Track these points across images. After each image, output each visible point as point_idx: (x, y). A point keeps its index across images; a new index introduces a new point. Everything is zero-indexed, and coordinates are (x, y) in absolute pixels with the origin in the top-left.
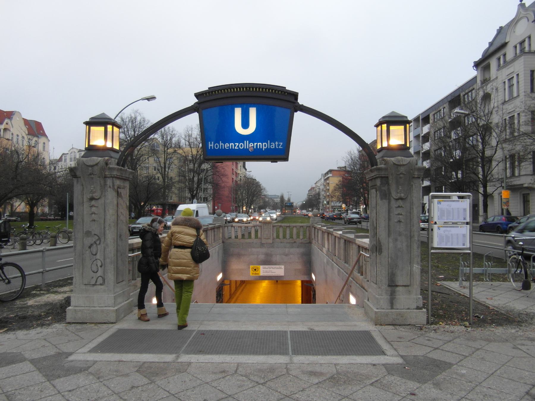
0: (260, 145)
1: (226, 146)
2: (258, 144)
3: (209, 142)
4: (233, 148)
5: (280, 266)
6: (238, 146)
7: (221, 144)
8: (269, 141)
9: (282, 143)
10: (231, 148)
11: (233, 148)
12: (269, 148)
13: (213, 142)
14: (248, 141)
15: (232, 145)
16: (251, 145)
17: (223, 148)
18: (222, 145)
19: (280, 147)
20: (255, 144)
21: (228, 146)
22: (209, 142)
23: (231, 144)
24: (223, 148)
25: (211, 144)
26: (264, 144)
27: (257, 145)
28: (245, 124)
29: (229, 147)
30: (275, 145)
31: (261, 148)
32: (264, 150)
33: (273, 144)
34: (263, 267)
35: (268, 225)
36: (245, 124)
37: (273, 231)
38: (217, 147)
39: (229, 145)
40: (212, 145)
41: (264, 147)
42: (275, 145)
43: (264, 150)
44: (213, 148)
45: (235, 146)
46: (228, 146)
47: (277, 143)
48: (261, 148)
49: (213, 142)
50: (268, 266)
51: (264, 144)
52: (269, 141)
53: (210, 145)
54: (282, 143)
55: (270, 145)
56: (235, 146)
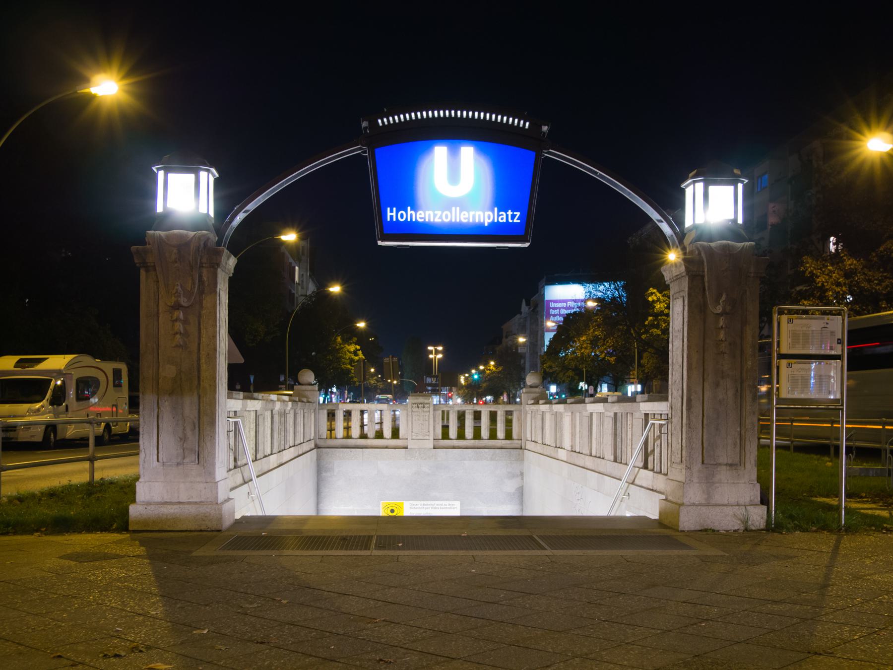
3: (389, 209)
5: (451, 503)
7: (409, 212)
9: (518, 214)
13: (395, 209)
14: (458, 209)
15: (429, 215)
18: (411, 215)
19: (515, 221)
20: (472, 213)
22: (389, 209)
25: (392, 211)
27: (474, 217)
30: (507, 216)
33: (502, 215)
34: (411, 505)
35: (424, 407)
37: (434, 421)
38: (402, 216)
39: (425, 213)
40: (394, 214)
42: (507, 216)
44: (394, 220)
45: (435, 215)
47: (510, 213)
49: (395, 209)
50: (422, 502)
53: (389, 214)
54: (518, 214)
55: (499, 216)
56: (435, 215)
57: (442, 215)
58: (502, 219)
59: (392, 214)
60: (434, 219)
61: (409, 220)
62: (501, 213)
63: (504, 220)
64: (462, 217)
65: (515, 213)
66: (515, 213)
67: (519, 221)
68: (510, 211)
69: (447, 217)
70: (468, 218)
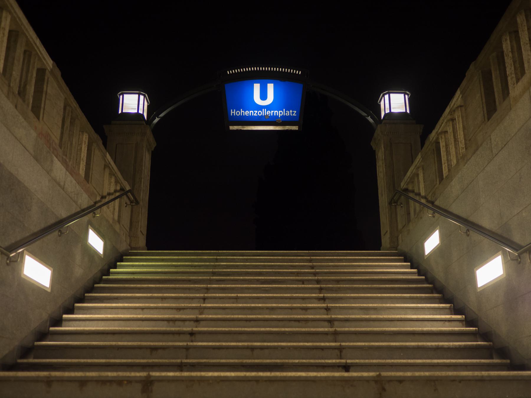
0: (276, 112)
1: (246, 113)
2: (275, 112)
3: (232, 110)
4: (253, 115)
7: (242, 112)
8: (284, 109)
9: (295, 112)
10: (250, 115)
11: (253, 115)
12: (284, 115)
13: (235, 110)
14: (265, 109)
15: (252, 113)
16: (269, 112)
17: (244, 115)
18: (243, 113)
19: (294, 115)
20: (272, 112)
22: (232, 110)
23: (250, 112)
24: (244, 115)
25: (233, 111)
26: (280, 112)
27: (273, 113)
28: (264, 96)
29: (249, 114)
30: (290, 113)
31: (277, 115)
32: (280, 117)
33: (288, 112)
36: (264, 96)
38: (238, 113)
40: (234, 112)
41: (280, 114)
42: (290, 113)
43: (280, 117)
44: (235, 115)
45: (254, 113)
46: (248, 113)
47: (291, 111)
48: (277, 115)
49: (235, 110)
51: (280, 112)
52: (284, 109)
53: (232, 112)
54: (295, 112)
55: (285, 113)
56: (254, 113)
57: (257, 113)
58: (287, 114)
60: (254, 114)
61: (241, 115)
62: (286, 111)
65: (294, 111)
66: (294, 111)
67: (296, 115)
68: (291, 110)
69: (260, 114)
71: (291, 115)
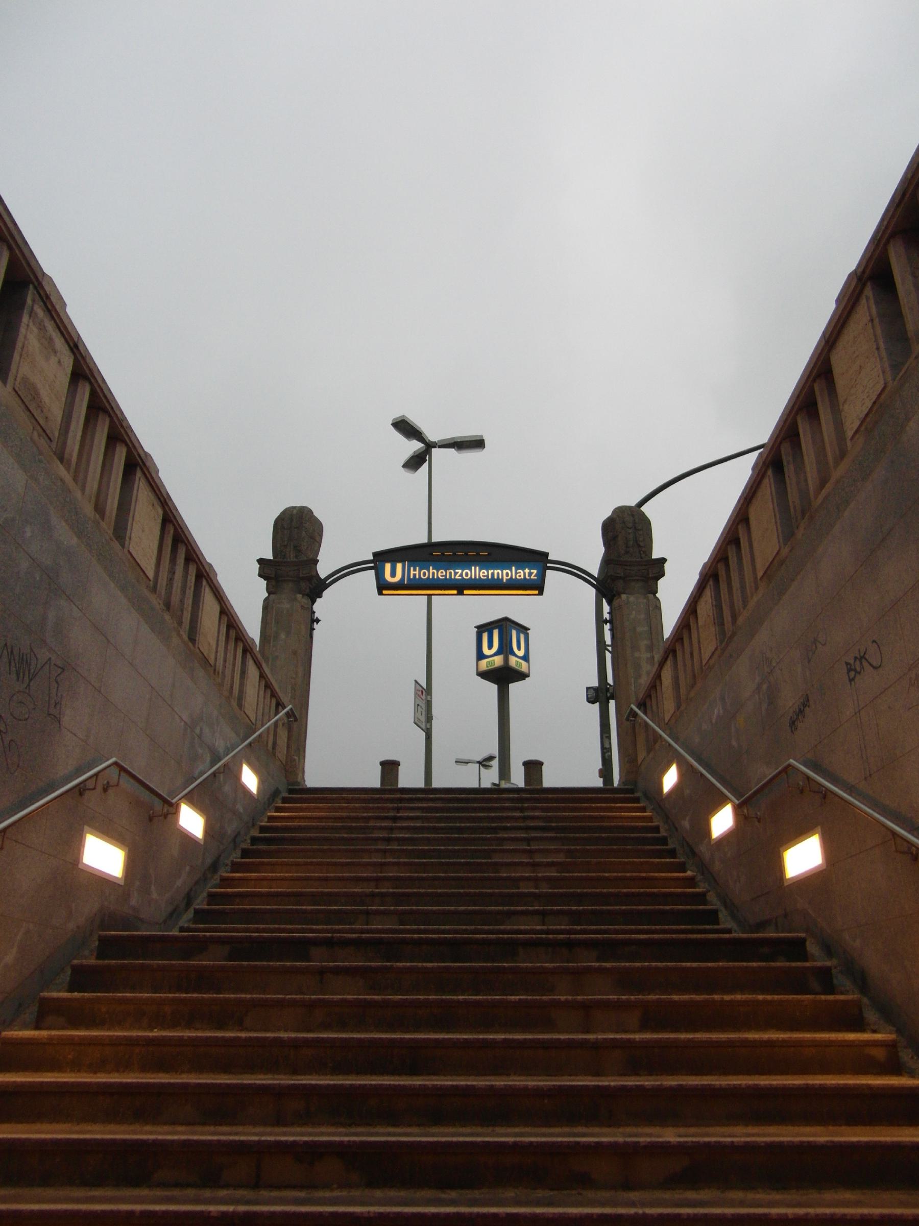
0: (498, 573)
2: (496, 572)
4: (453, 577)
6: (461, 575)
7: (431, 571)
8: (513, 568)
9: (535, 571)
10: (448, 577)
12: (514, 577)
13: (417, 568)
14: (477, 568)
15: (450, 573)
17: (436, 577)
18: (433, 573)
19: (532, 577)
20: (490, 572)
21: (444, 574)
23: (448, 572)
24: (436, 577)
25: (415, 570)
27: (493, 574)
31: (500, 577)
32: (505, 581)
33: (520, 573)
40: (417, 572)
44: (417, 577)
45: (456, 574)
46: (444, 574)
48: (500, 577)
49: (417, 568)
51: (505, 572)
54: (535, 571)
55: (516, 573)
56: (456, 574)
59: (415, 572)
60: (455, 576)
61: (431, 577)
62: (518, 571)
63: (522, 577)
64: (481, 574)
65: (532, 571)
66: (532, 571)
70: (488, 576)
71: (527, 577)
